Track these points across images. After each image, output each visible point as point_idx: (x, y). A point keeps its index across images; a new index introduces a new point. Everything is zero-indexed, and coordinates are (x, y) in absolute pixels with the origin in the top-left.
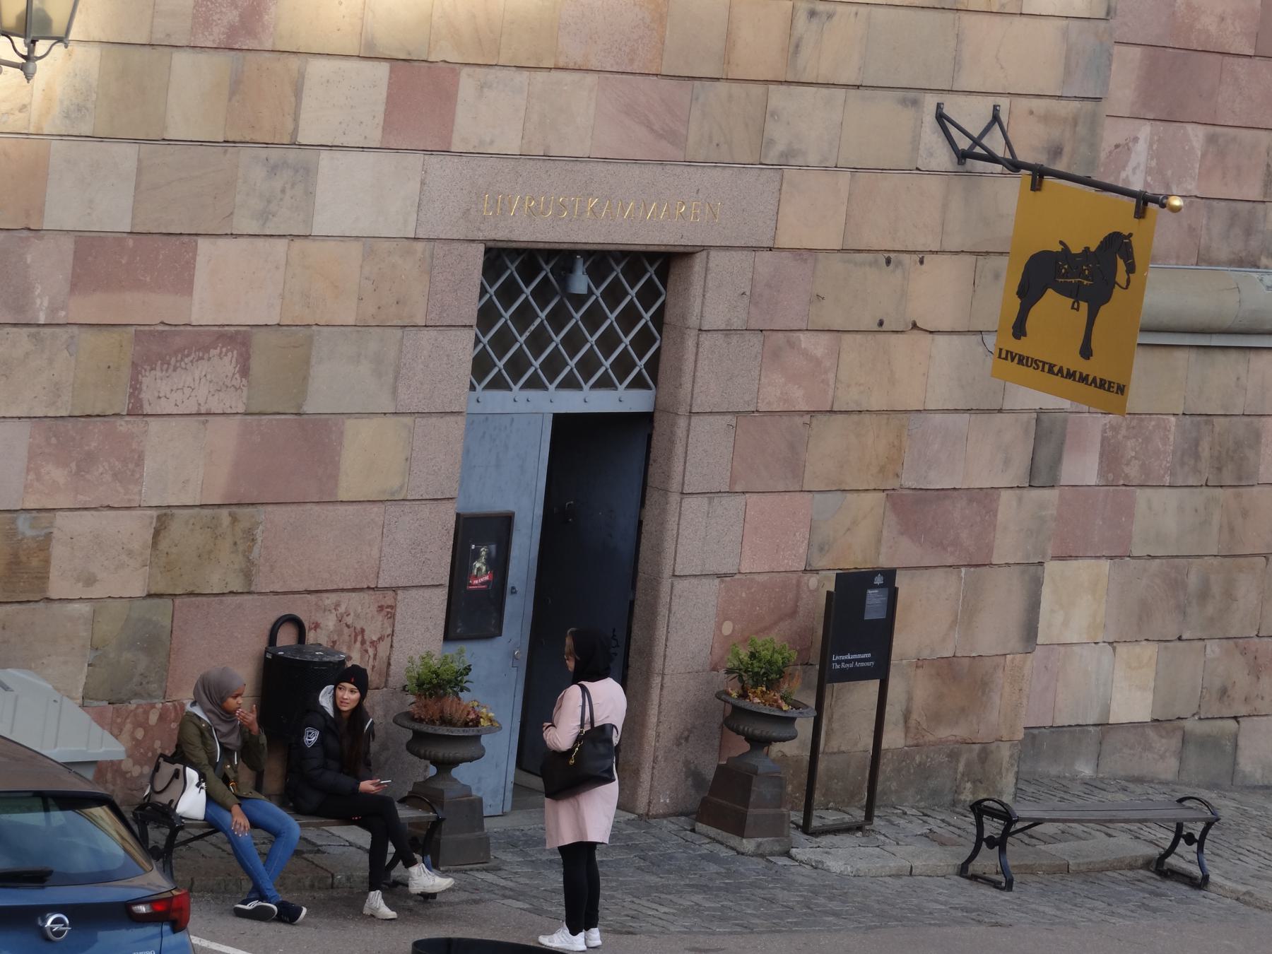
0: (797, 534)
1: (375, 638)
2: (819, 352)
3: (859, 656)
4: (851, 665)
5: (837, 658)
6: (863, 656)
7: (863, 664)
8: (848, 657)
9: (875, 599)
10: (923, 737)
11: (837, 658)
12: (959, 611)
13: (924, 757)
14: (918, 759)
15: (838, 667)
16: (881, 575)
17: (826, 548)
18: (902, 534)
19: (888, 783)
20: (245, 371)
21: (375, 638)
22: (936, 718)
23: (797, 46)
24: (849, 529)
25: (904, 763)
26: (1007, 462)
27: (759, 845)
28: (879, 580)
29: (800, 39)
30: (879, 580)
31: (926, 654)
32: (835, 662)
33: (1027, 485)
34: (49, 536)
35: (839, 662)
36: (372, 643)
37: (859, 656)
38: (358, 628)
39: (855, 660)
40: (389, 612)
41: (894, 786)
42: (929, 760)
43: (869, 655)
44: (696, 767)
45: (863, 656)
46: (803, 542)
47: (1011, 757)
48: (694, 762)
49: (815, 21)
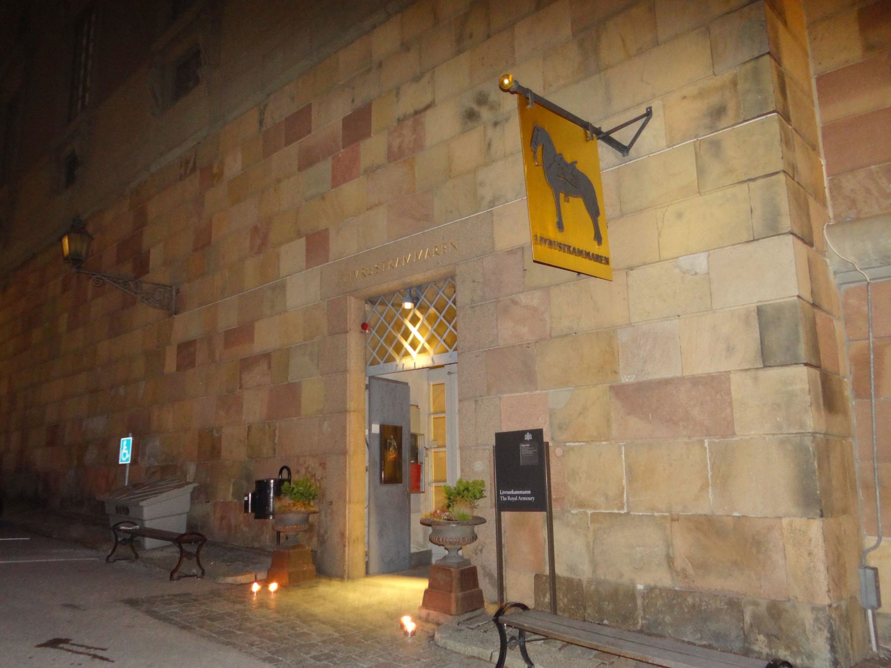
0: (540, 419)
1: (319, 478)
2: (535, 302)
3: (521, 492)
4: (516, 499)
5: (504, 492)
6: (525, 492)
7: (525, 499)
8: (512, 492)
9: (525, 450)
10: (693, 582)
11: (504, 492)
12: (709, 476)
13: (697, 599)
14: (690, 600)
15: (505, 499)
16: (530, 433)
17: (564, 427)
18: (629, 414)
19: (661, 616)
20: (270, 368)
21: (319, 478)
22: (702, 567)
23: (489, 145)
24: (580, 414)
25: (675, 602)
26: (730, 350)
27: (428, 615)
28: (528, 437)
29: (491, 140)
30: (528, 437)
31: (677, 509)
32: (502, 495)
33: (762, 366)
34: (221, 436)
35: (506, 496)
36: (318, 480)
37: (521, 492)
38: (313, 473)
39: (518, 495)
40: (323, 465)
41: (668, 619)
42: (704, 604)
43: (529, 492)
44: (490, 571)
45: (525, 492)
46: (545, 424)
47: (817, 619)
48: (487, 567)
49: (498, 128)
